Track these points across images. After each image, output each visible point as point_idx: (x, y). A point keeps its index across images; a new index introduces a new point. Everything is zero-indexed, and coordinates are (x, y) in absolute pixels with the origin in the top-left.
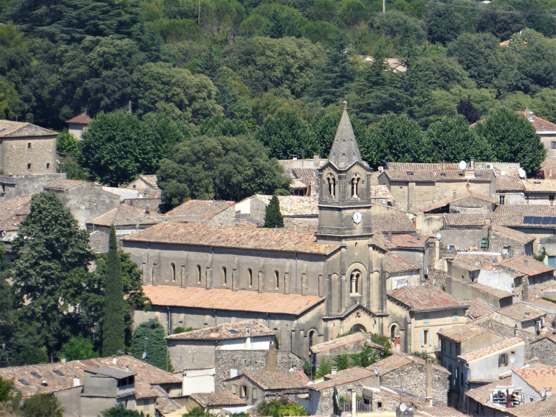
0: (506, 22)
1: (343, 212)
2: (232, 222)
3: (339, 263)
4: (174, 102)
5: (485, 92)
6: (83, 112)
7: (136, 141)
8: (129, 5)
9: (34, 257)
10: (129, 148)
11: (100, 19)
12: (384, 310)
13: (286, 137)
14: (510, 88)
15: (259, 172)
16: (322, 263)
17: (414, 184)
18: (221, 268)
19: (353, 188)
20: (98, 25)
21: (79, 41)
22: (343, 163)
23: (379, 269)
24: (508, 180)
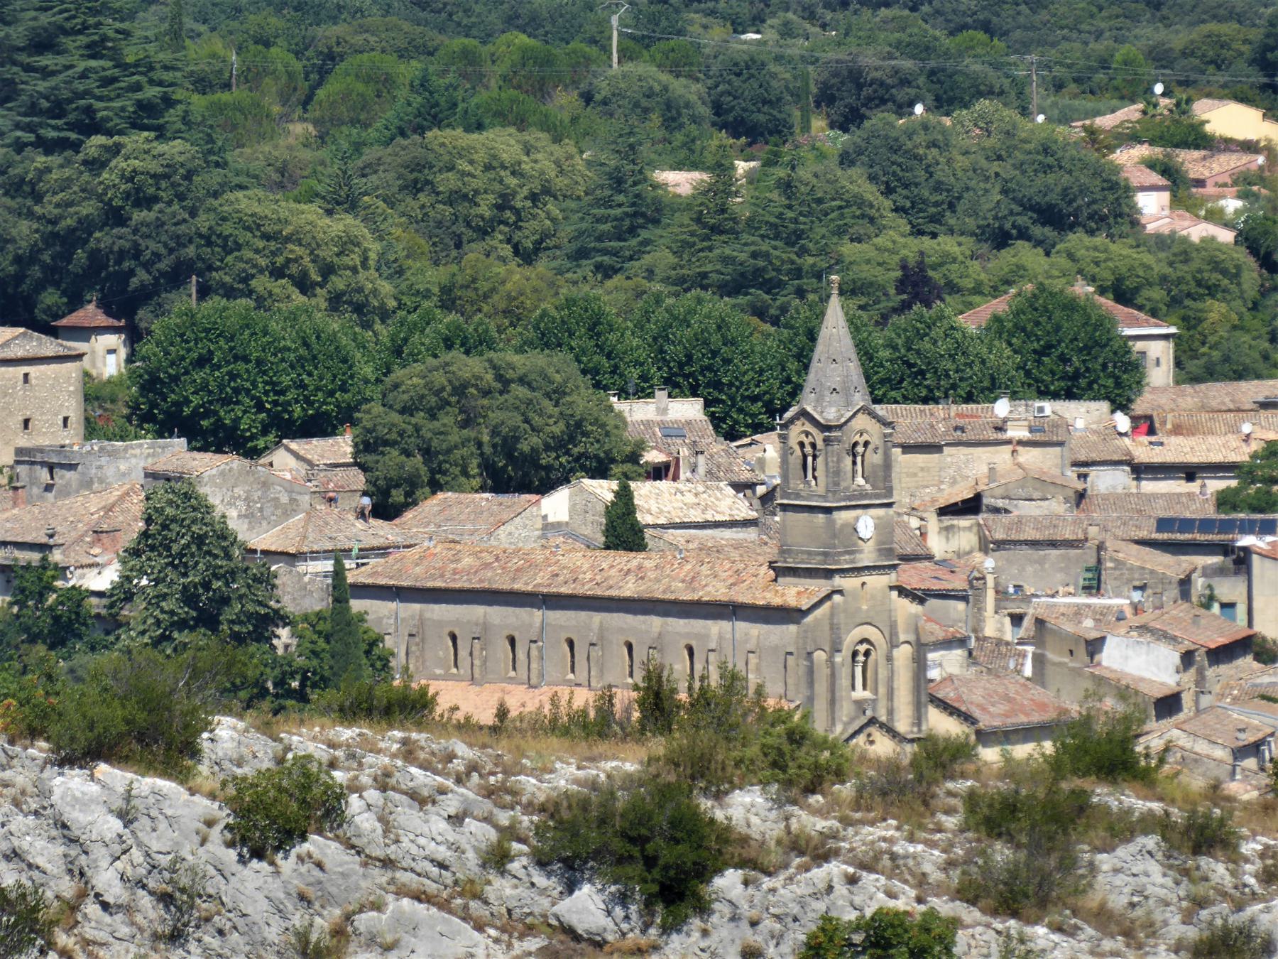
0: (882, 84)
1: (836, 515)
2: (535, 541)
3: (827, 628)
4: (290, 277)
5: (948, 244)
6: (90, 302)
7: (259, 362)
8: (158, 66)
9: (158, 623)
10: (243, 380)
11: (100, 99)
12: (924, 727)
13: (584, 352)
14: (983, 233)
15: (576, 429)
16: (793, 628)
17: (899, 450)
18: (622, 643)
19: (854, 463)
20: (95, 111)
21: (76, 146)
22: (833, 410)
23: (912, 638)
24: (1094, 438)
